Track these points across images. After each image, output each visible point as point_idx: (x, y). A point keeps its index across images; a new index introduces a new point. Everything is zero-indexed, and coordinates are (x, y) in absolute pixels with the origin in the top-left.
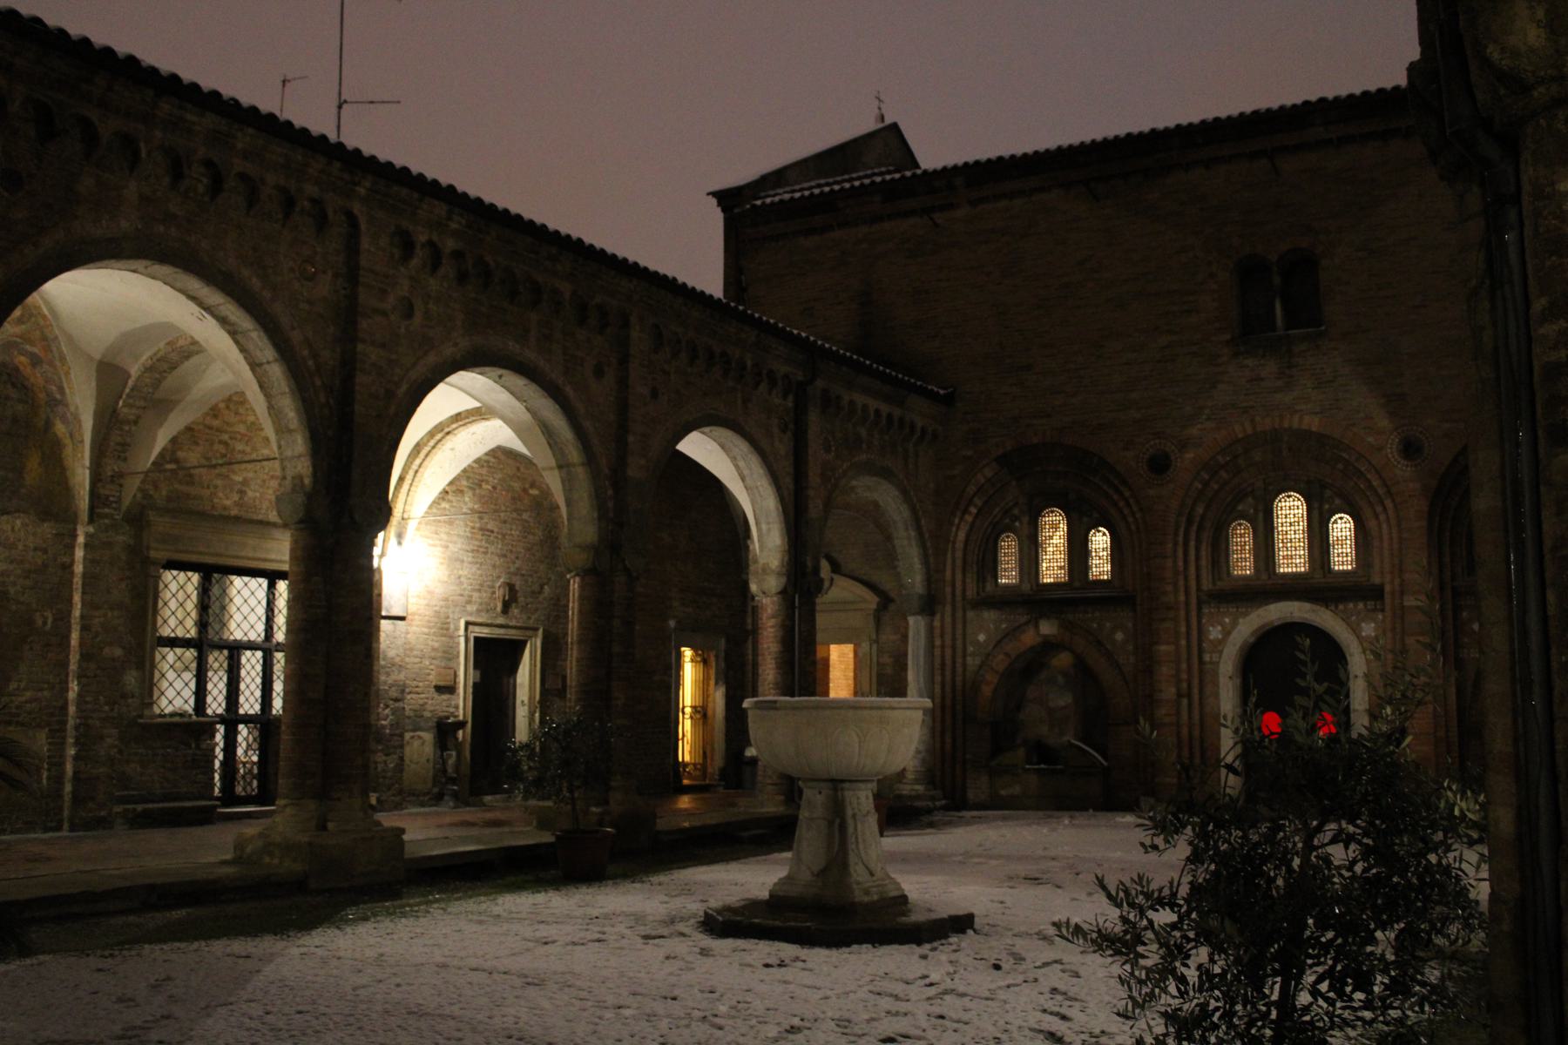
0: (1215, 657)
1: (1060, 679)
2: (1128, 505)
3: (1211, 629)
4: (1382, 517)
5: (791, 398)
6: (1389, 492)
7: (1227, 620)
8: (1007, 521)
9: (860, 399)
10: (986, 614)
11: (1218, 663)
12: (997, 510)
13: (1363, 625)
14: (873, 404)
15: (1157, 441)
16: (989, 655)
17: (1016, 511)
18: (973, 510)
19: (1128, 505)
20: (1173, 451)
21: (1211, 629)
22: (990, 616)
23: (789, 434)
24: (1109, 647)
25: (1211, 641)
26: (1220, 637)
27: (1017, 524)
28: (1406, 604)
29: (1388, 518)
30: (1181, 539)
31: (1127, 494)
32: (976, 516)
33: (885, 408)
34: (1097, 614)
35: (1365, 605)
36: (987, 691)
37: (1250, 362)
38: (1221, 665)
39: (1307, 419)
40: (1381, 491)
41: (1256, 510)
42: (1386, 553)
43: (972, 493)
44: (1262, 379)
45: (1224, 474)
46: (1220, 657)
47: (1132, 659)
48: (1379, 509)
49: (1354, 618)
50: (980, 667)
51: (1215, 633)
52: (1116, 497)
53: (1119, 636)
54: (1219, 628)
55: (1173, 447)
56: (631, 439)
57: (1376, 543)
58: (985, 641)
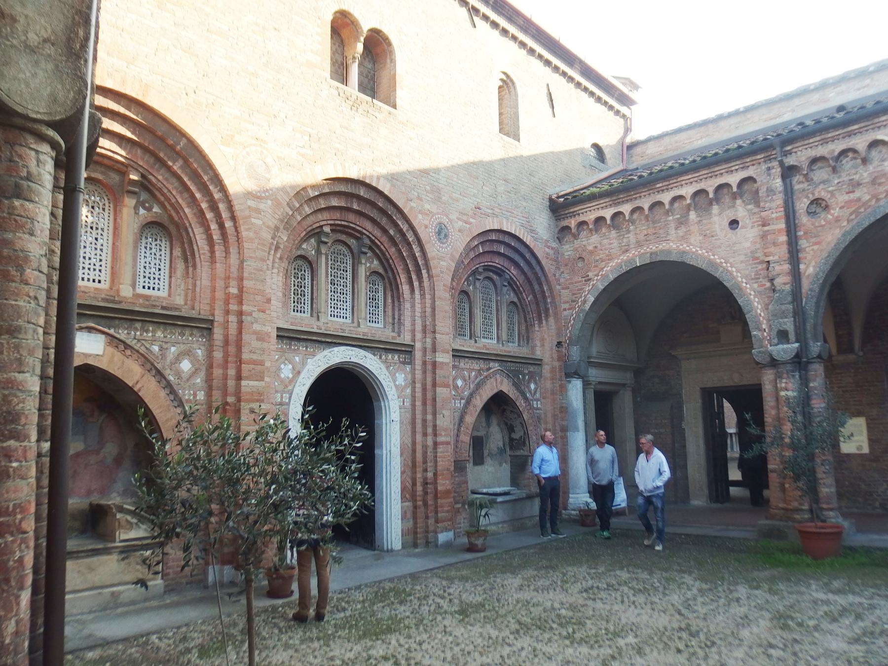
2: (214, 207)
3: (282, 366)
7: (297, 359)
11: (288, 404)
13: (397, 375)
19: (214, 207)
24: (171, 378)
25: (282, 381)
26: (291, 376)
28: (437, 359)
34: (159, 334)
35: (399, 357)
38: (291, 406)
41: (318, 252)
46: (290, 398)
48: (414, 277)
49: (391, 368)
51: (286, 371)
57: (408, 305)
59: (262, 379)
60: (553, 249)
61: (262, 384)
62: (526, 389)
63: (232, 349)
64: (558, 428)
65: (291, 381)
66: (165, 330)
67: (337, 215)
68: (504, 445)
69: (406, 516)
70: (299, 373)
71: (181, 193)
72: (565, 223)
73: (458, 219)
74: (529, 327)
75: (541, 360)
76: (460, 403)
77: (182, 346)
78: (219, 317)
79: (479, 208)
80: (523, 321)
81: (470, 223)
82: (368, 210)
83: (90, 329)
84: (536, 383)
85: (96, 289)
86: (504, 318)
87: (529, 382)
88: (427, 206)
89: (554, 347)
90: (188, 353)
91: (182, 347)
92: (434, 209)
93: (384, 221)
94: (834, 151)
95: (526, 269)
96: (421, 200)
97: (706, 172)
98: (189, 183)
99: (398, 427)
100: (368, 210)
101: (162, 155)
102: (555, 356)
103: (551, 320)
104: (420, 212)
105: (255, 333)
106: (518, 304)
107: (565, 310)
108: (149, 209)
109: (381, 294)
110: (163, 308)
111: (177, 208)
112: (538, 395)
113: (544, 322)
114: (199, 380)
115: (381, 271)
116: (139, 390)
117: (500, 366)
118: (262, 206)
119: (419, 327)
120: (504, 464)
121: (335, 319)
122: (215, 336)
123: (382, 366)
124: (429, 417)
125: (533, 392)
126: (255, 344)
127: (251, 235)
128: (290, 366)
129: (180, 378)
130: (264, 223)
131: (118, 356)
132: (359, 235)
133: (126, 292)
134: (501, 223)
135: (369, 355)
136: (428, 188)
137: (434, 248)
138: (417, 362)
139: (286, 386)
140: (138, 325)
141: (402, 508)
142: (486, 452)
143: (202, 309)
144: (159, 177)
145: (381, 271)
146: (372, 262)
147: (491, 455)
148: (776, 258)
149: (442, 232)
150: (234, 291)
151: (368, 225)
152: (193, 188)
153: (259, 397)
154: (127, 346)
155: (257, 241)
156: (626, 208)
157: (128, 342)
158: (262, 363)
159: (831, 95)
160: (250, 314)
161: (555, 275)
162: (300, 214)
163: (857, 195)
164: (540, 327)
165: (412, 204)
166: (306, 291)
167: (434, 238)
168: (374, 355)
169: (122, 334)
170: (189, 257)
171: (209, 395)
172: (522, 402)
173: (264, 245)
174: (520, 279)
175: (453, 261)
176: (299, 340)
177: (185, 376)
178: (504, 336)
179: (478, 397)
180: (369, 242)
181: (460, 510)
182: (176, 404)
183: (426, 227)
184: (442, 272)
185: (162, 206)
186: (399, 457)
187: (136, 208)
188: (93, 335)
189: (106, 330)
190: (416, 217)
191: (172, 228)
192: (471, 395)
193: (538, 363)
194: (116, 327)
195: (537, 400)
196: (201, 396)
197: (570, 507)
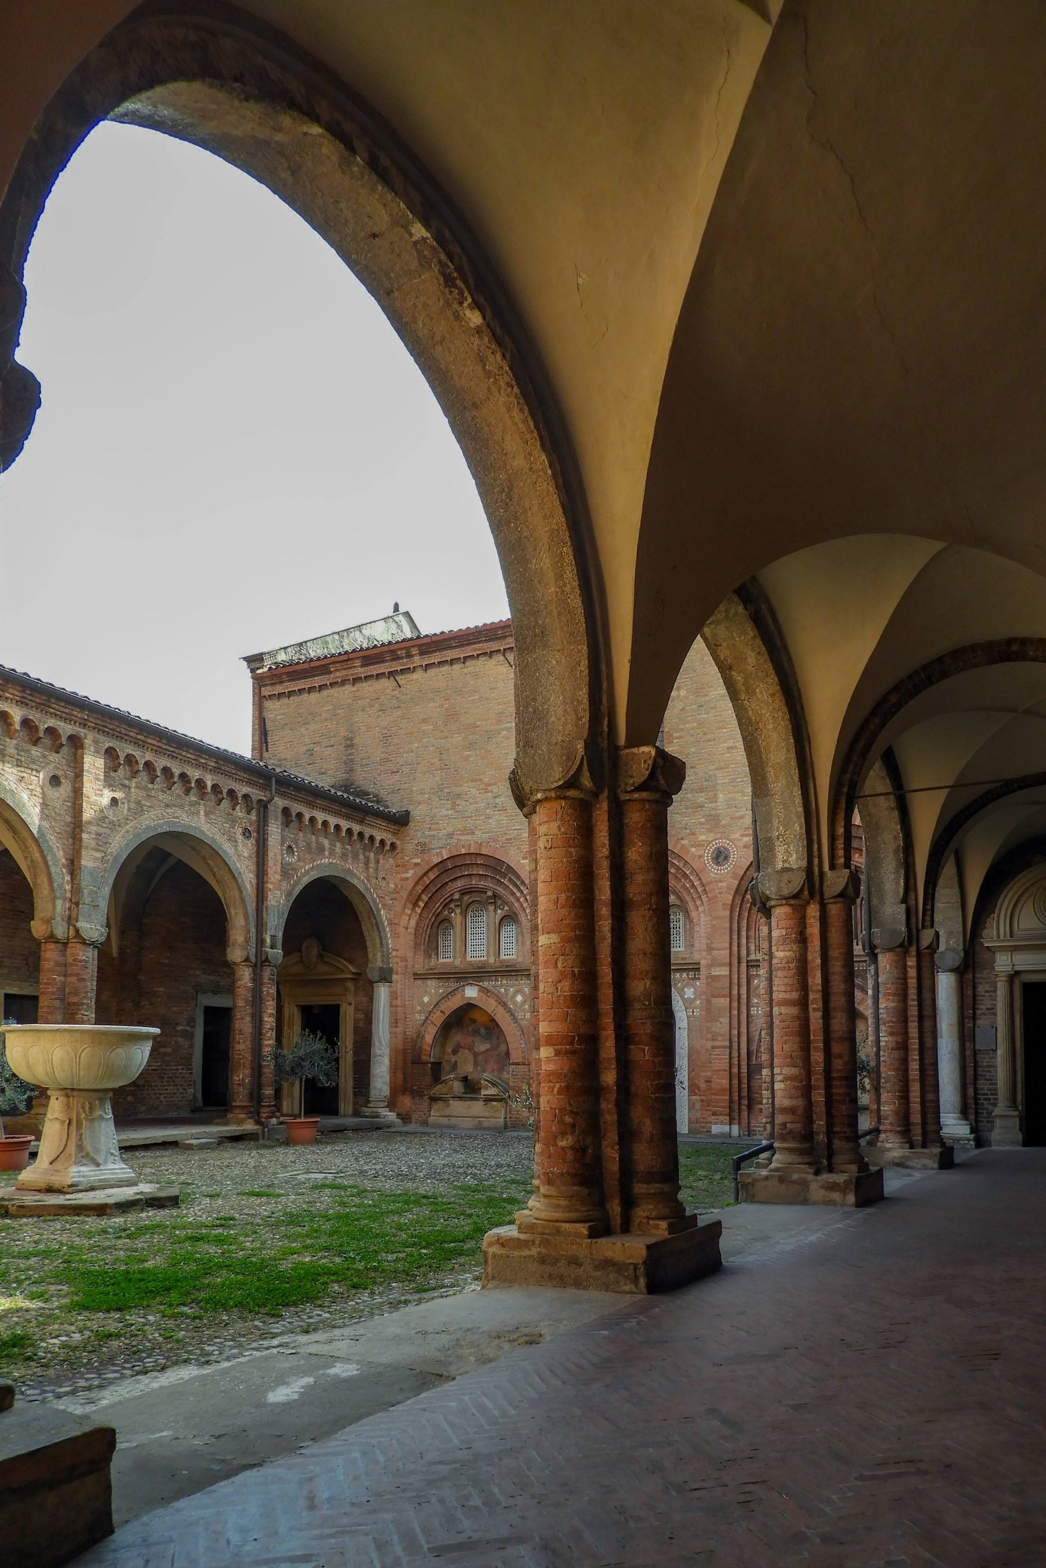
1: (483, 1031)
5: (254, 813)
6: (705, 890)
8: (446, 912)
9: (320, 816)
10: (429, 982)
14: (333, 821)
17: (452, 906)
18: (422, 904)
22: (432, 984)
23: (253, 840)
27: (453, 914)
32: (423, 909)
33: (345, 825)
34: (504, 982)
36: (429, 1038)
47: (528, 1015)
50: (425, 1021)
52: (518, 894)
53: (519, 998)
56: (84, 836)
73: (743, 835)
88: (703, 837)
91: (517, 988)
104: (692, 846)
108: (502, 909)
110: (507, 966)
129: (516, 1006)
133: (492, 960)
136: (703, 820)
140: (493, 978)
149: (720, 856)
152: (515, 891)
154: (488, 991)
167: (711, 866)
169: (485, 984)
175: (735, 879)
183: (700, 857)
185: (508, 906)
187: (495, 910)
190: (688, 852)
191: (514, 916)
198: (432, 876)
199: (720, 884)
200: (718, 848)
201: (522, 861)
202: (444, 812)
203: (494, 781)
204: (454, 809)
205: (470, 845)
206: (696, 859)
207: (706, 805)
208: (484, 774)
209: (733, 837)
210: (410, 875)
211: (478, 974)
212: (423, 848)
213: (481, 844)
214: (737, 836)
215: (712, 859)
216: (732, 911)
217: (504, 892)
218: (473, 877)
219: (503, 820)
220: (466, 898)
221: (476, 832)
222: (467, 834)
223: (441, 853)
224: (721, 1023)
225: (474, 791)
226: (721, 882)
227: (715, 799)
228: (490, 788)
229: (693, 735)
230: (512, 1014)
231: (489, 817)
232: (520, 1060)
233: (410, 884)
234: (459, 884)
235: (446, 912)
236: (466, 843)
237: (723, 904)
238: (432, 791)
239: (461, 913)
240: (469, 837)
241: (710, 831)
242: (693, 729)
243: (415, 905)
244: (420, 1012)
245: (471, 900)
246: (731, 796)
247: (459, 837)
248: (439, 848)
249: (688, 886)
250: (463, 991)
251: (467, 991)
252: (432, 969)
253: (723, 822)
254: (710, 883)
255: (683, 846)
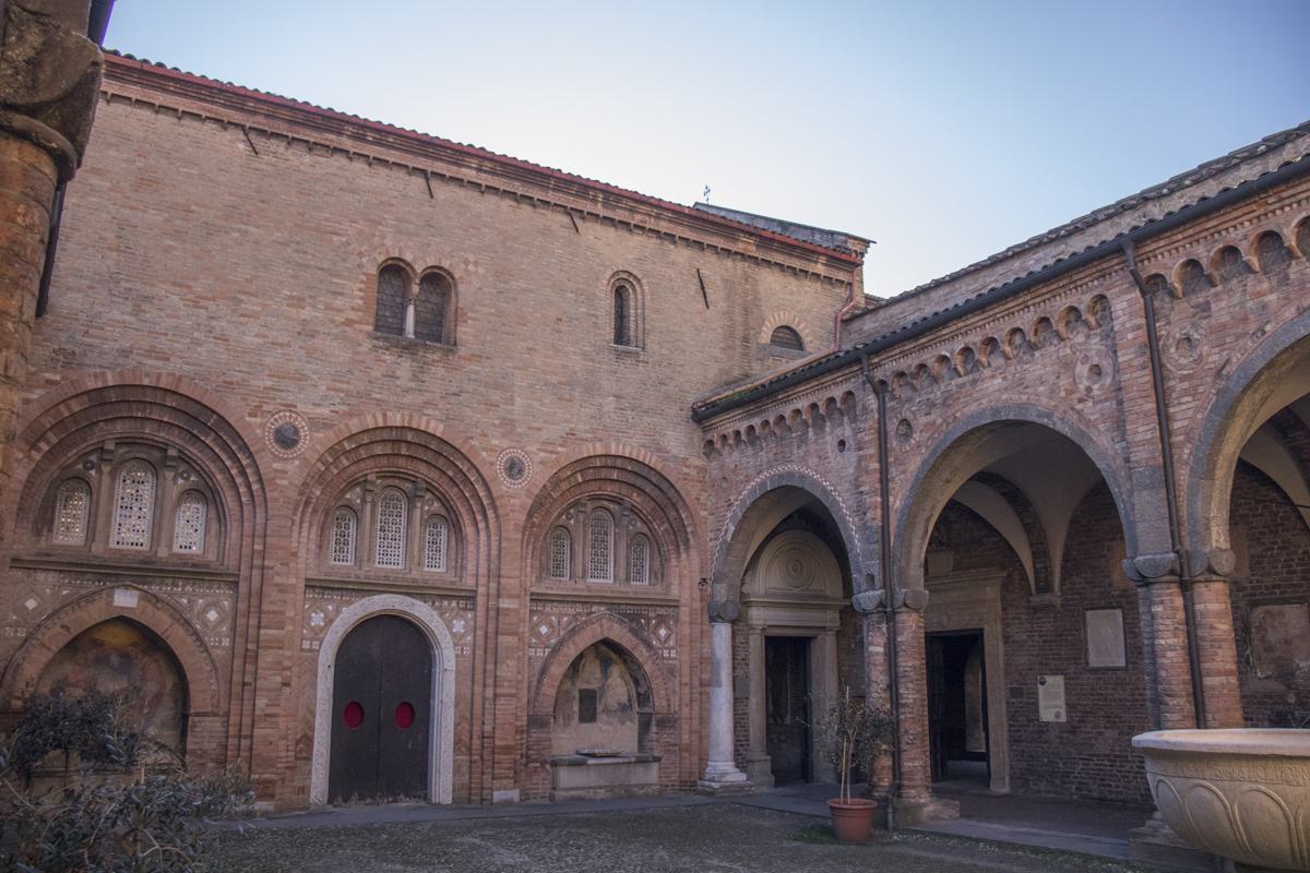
0: (315, 645)
1: (115, 660)
2: (243, 472)
4: (482, 525)
6: (493, 504)
7: (330, 607)
8: (80, 466)
10: (41, 576)
11: (318, 651)
12: (75, 451)
15: (288, 414)
16: (39, 626)
17: (93, 458)
18: (45, 447)
19: (243, 472)
20: (303, 427)
21: (313, 615)
22: (47, 581)
25: (312, 629)
26: (322, 624)
27: (93, 472)
28: (501, 606)
29: (487, 527)
30: (297, 519)
31: (244, 463)
35: (458, 604)
37: (388, 357)
38: (321, 653)
39: (433, 424)
40: (485, 502)
41: (364, 500)
42: (483, 557)
43: (48, 426)
44: (398, 378)
45: (345, 462)
46: (320, 645)
48: (479, 518)
51: (317, 619)
53: (212, 615)
54: (322, 615)
55: (304, 424)
57: (471, 548)
58: (34, 609)
59: (283, 628)
60: (695, 467)
61: (283, 632)
62: (652, 636)
63: (254, 601)
64: (696, 682)
65: (322, 629)
66: (194, 584)
67: (384, 461)
68: (629, 700)
69: (459, 771)
70: (331, 621)
71: (214, 462)
72: (709, 437)
74: (664, 561)
75: (678, 601)
76: (544, 652)
77: (210, 599)
78: (244, 572)
79: (573, 434)
80: (656, 555)
81: (558, 453)
82: (420, 453)
83: (127, 587)
84: (668, 628)
85: (136, 551)
86: (623, 552)
87: (657, 627)
88: (495, 442)
89: (696, 586)
90: (215, 605)
92: (505, 443)
93: (441, 463)
94: (910, 366)
95: (655, 493)
96: (484, 435)
97: (816, 383)
98: (220, 453)
99: (454, 674)
100: (420, 453)
101: (195, 432)
102: (697, 595)
103: (694, 554)
104: (484, 449)
105: (277, 585)
106: (649, 535)
107: (711, 540)
108: (187, 479)
109: (444, 537)
110: (194, 565)
111: (211, 476)
112: (671, 643)
113: (684, 556)
114: (224, 629)
115: (444, 513)
116: (168, 637)
117: (608, 609)
118: (289, 467)
119: (483, 570)
120: (628, 723)
121: (385, 566)
122: (240, 589)
123: (435, 613)
124: (490, 667)
125: (663, 640)
126: (275, 595)
127: (276, 494)
128: (322, 615)
130: (290, 483)
131: (150, 608)
132: (414, 479)
133: (163, 553)
134: (608, 446)
135: (418, 603)
136: (497, 422)
137: (504, 485)
138: (479, 608)
139: (317, 634)
140: (169, 581)
141: (454, 761)
142: (600, 708)
143: (231, 563)
144: (193, 450)
145: (444, 513)
146: (432, 505)
147: (607, 711)
148: (867, 488)
149: (514, 469)
150: (258, 547)
151: (423, 468)
152: (224, 457)
153: (278, 644)
154: (158, 600)
155: (282, 500)
156: (756, 421)
157: (161, 595)
158: (283, 613)
159: (1031, 262)
160: (272, 568)
161: (698, 499)
162: (336, 467)
163: (932, 417)
164: (678, 562)
165: (473, 442)
166: (350, 539)
167: (502, 476)
168: (425, 602)
169: (154, 589)
170: (221, 518)
171: (233, 642)
172: (644, 650)
173: (289, 503)
174: (646, 507)
175: (529, 497)
176: (332, 589)
177: (211, 625)
178: (622, 575)
179: (571, 646)
180: (424, 486)
181: (539, 770)
182: (202, 649)
183: (492, 464)
184: (513, 511)
186: (452, 709)
187: (175, 479)
188: (129, 592)
189: (140, 587)
190: (479, 455)
191: (209, 495)
192: (561, 643)
193: (675, 605)
194: (150, 584)
195: (670, 649)
196: (226, 642)
197: (707, 777)
198: (76, 407)
199: (512, 501)
200: (511, 459)
201: (248, 419)
202: (116, 315)
203: (210, 295)
204: (136, 315)
205: (159, 376)
206: (488, 466)
207: (502, 406)
208: (196, 279)
209: (528, 448)
210: (35, 397)
211: (141, 570)
212: (68, 359)
213: (180, 378)
214: (534, 449)
215: (506, 469)
216: (523, 534)
217: (199, 455)
218: (148, 424)
219: (222, 353)
220: (121, 451)
221: (172, 359)
222: (157, 358)
223: (103, 374)
224: (508, 666)
225: (176, 299)
226: (514, 498)
227: (511, 401)
228: (203, 303)
229: (490, 322)
230: (199, 639)
231: (198, 343)
232: (209, 709)
233: (35, 410)
234: (120, 428)
235: (80, 466)
236: (153, 371)
237: (515, 524)
238: (97, 277)
239: (110, 473)
240: (161, 363)
241: (504, 436)
242: (491, 314)
243: (34, 446)
244: (16, 625)
245: (131, 455)
246: (529, 402)
247: (139, 359)
248: (101, 367)
249: (467, 495)
250: (111, 595)
251: (116, 596)
252: (48, 555)
253: (519, 430)
254: (502, 497)
255: (472, 446)
